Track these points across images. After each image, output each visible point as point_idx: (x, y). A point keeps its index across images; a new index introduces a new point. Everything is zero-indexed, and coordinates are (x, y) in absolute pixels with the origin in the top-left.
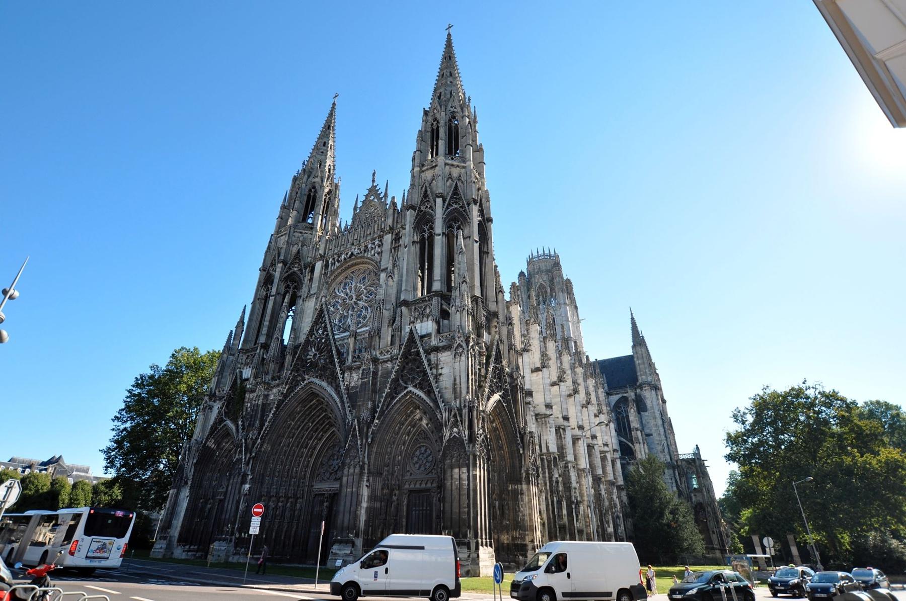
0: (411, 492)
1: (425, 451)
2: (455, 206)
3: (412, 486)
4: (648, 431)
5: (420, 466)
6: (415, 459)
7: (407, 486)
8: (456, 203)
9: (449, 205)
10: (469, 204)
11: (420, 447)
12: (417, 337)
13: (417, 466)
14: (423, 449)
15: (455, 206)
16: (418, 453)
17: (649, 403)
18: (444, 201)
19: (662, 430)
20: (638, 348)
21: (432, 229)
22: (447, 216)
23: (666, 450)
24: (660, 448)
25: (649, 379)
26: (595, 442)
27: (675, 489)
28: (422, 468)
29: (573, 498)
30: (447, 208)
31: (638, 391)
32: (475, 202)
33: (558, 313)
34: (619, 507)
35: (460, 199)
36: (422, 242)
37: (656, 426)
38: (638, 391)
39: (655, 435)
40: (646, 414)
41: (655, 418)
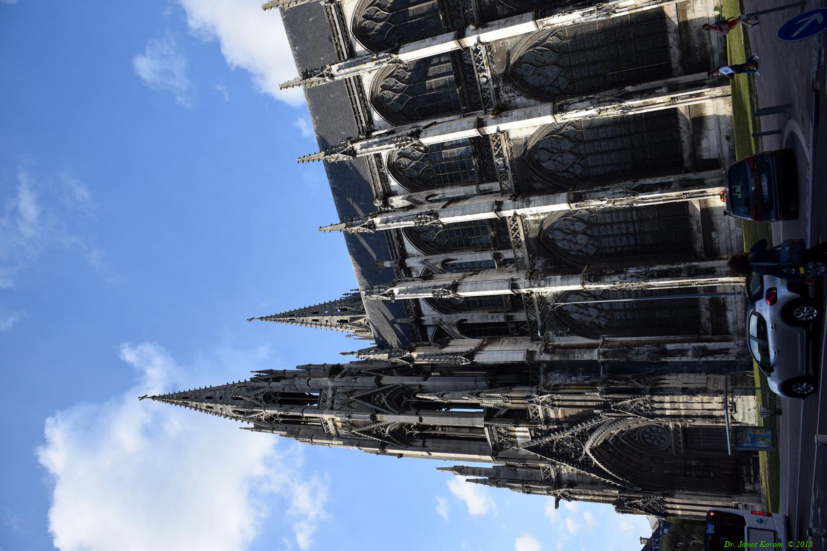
0: (686, 447)
1: (647, 433)
2: (384, 399)
3: (682, 446)
5: (662, 438)
6: (655, 443)
7: (682, 451)
8: (379, 399)
9: (383, 406)
10: (380, 385)
11: (643, 438)
12: (536, 443)
13: (662, 441)
14: (645, 435)
15: (384, 399)
16: (649, 441)
18: (378, 412)
21: (410, 425)
22: (396, 409)
28: (664, 436)
30: (387, 409)
32: (378, 379)
35: (375, 394)
36: (424, 437)
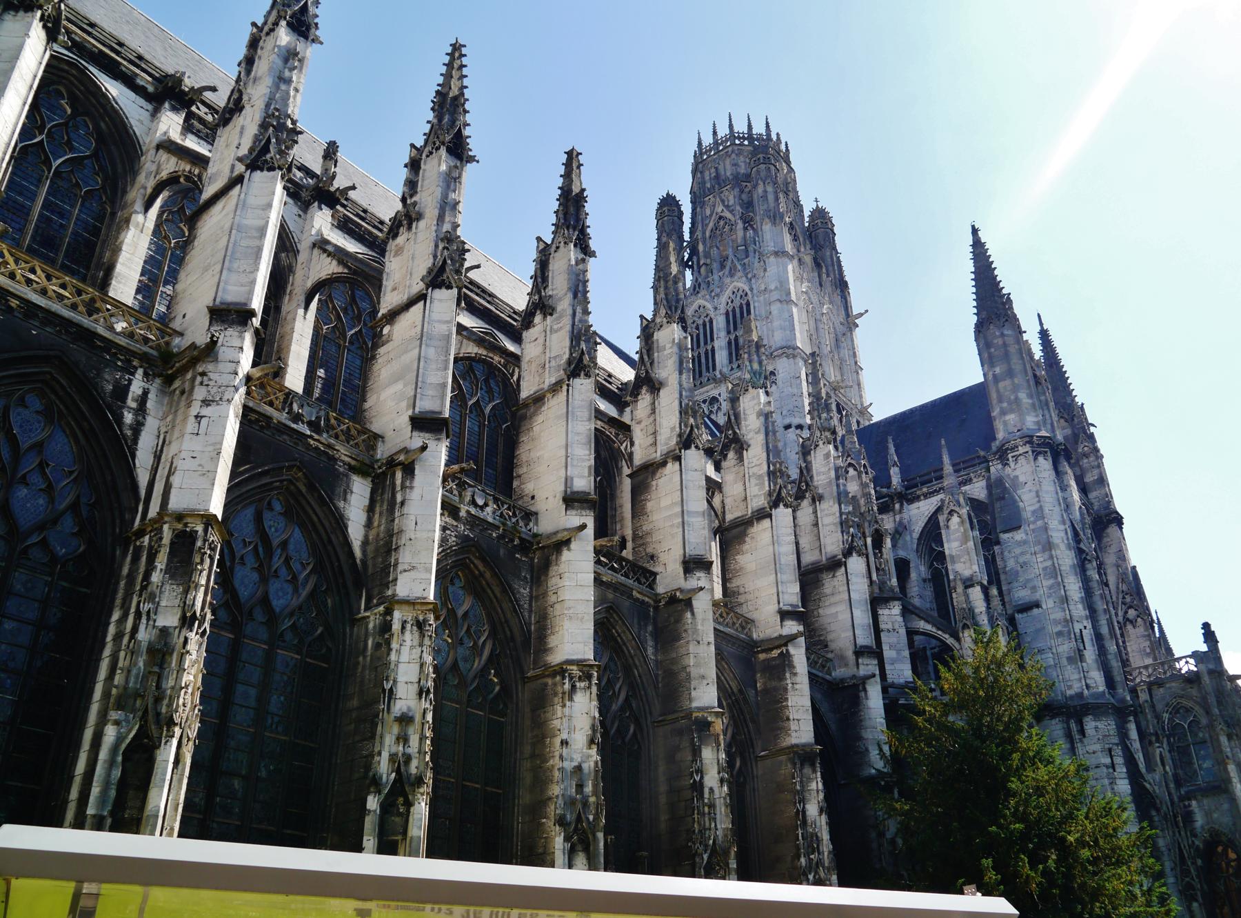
4: (1021, 595)
17: (1026, 500)
19: (1074, 587)
20: (994, 331)
23: (1090, 653)
24: (1065, 648)
25: (1031, 421)
26: (698, 579)
27: (1124, 786)
29: (383, 766)
31: (996, 467)
33: (759, 285)
34: (826, 846)
37: (1054, 572)
38: (996, 467)
39: (1048, 603)
40: (1019, 536)
41: (1049, 546)
